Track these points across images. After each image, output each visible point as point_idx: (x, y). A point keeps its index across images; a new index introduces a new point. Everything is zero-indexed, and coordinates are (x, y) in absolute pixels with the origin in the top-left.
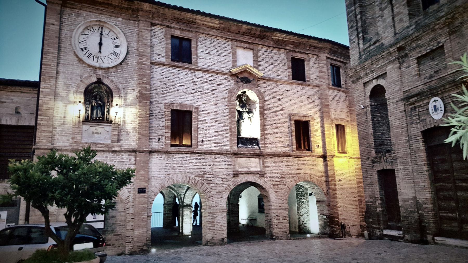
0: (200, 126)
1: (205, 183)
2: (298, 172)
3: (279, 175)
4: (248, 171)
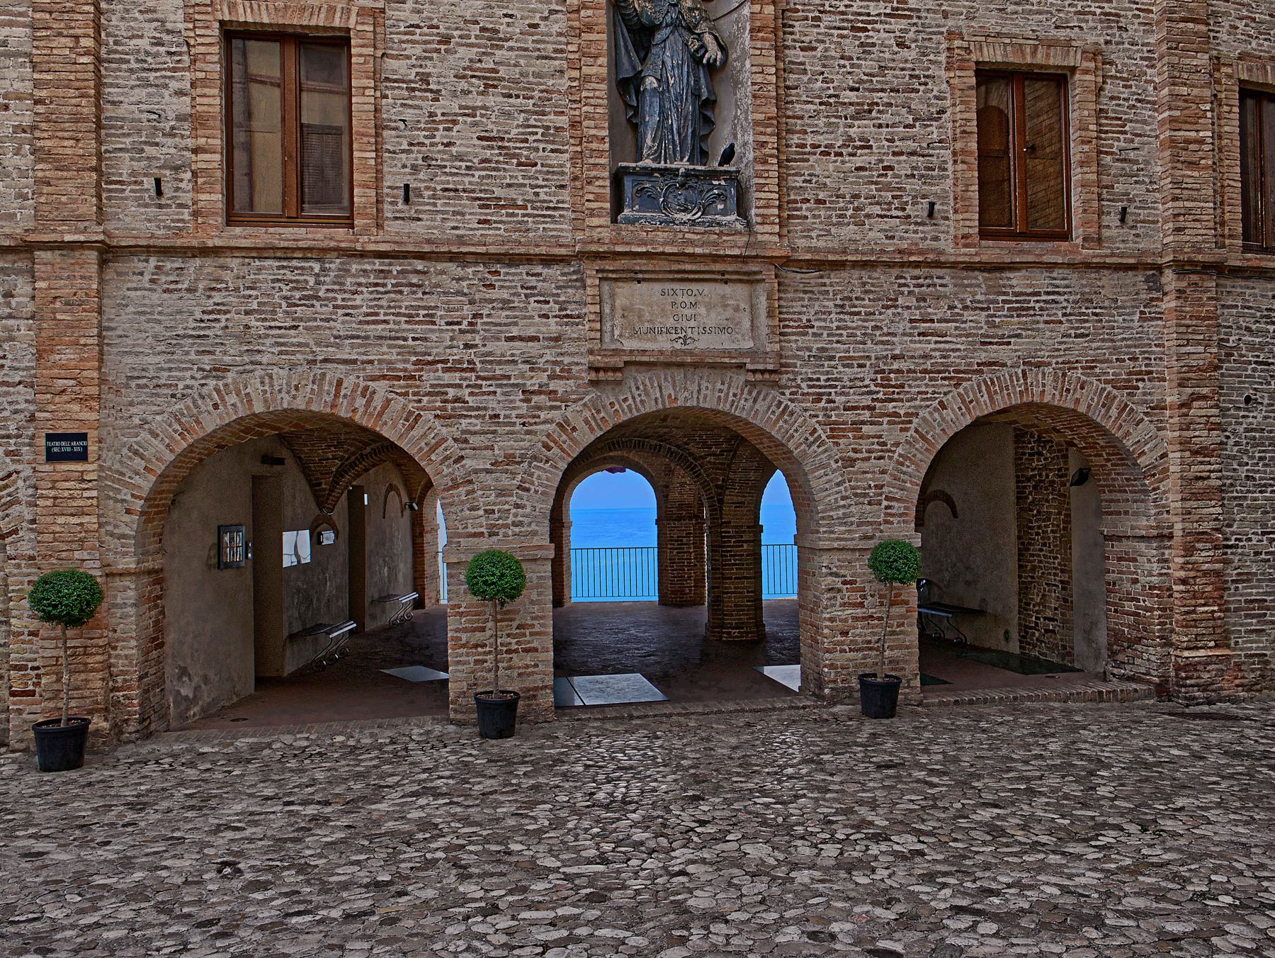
0: (391, 111)
1: (427, 415)
2: (983, 356)
3: (867, 374)
4: (675, 352)
